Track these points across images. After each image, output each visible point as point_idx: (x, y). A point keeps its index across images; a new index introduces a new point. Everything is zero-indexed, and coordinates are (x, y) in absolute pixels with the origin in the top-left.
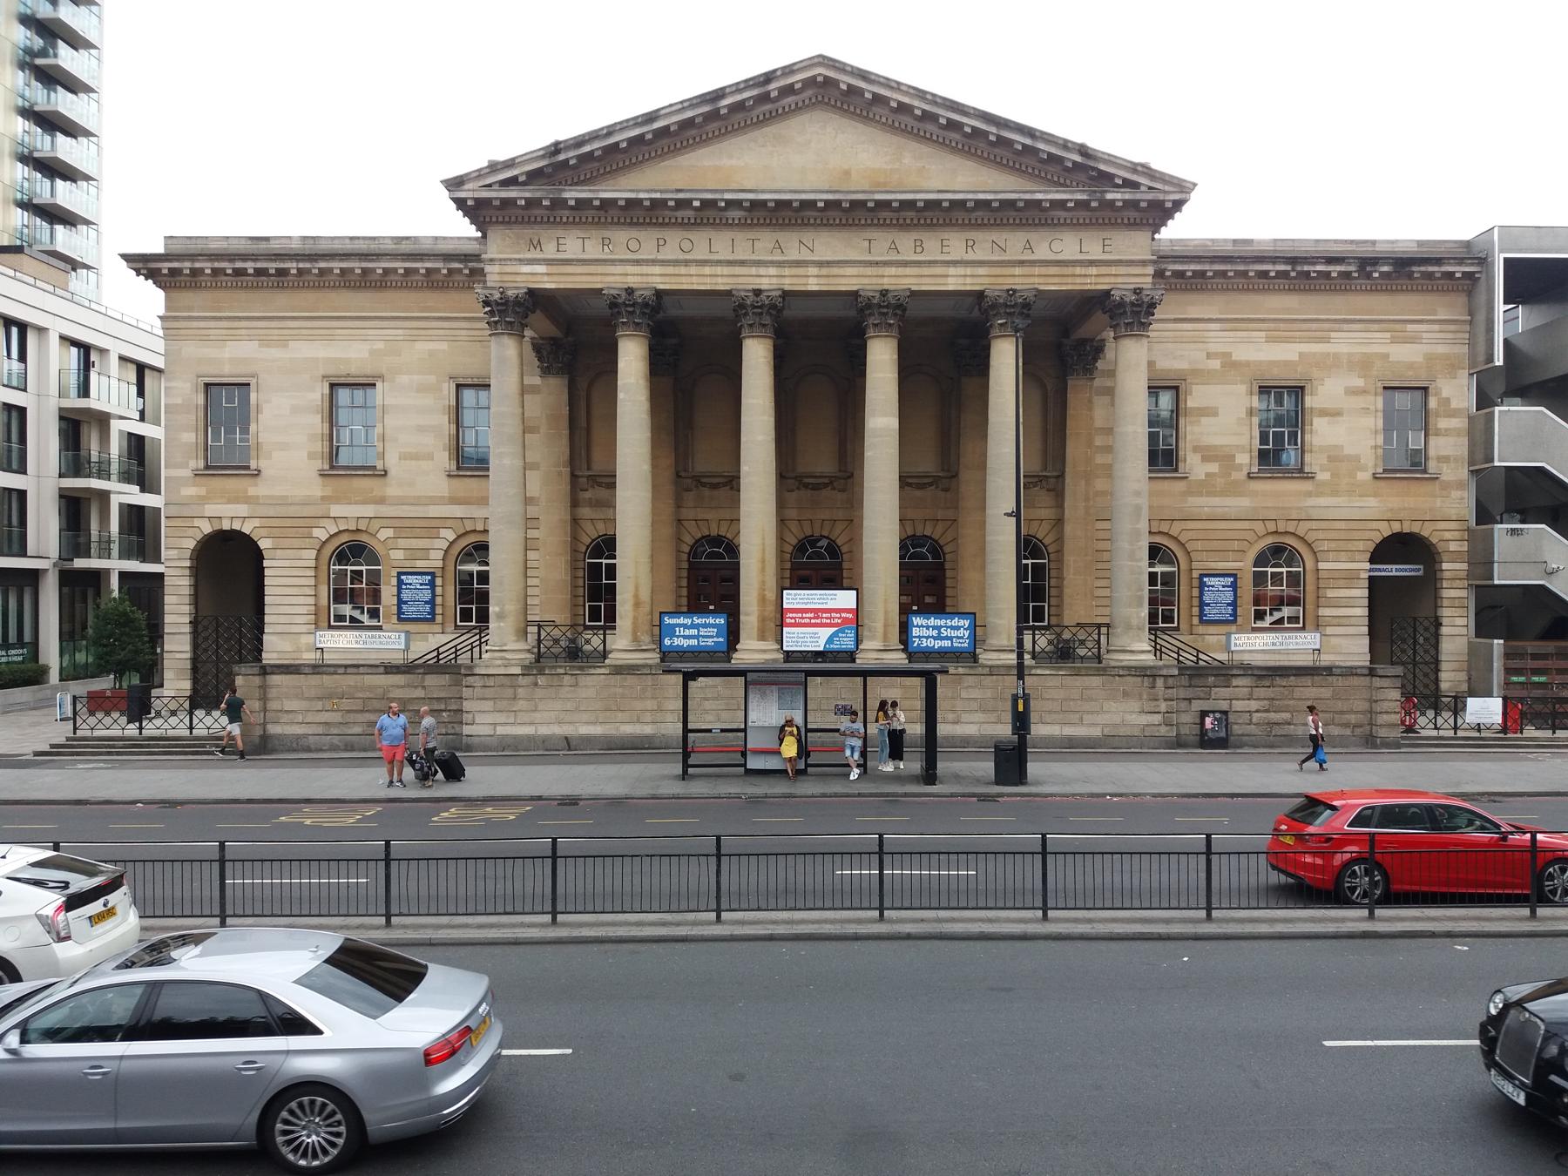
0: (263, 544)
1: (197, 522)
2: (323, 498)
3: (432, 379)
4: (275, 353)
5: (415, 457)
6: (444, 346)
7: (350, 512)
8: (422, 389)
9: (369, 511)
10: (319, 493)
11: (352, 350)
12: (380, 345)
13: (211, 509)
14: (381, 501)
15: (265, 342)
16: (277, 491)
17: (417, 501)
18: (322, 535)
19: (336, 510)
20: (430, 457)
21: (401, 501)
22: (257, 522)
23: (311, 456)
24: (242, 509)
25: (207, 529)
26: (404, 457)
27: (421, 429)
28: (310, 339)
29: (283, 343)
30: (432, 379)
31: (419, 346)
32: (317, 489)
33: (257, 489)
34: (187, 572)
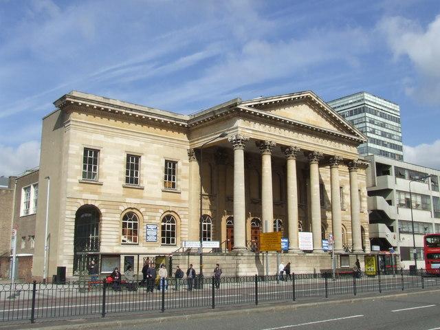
0: (102, 211)
1: (79, 201)
2: (123, 195)
3: (158, 157)
4: (110, 140)
5: (153, 183)
6: (162, 146)
7: (132, 201)
8: (155, 160)
9: (138, 201)
10: (122, 193)
11: (135, 145)
12: (143, 143)
13: (85, 196)
14: (142, 198)
15: (106, 135)
16: (109, 191)
17: (153, 199)
18: (122, 209)
19: (128, 200)
20: (157, 184)
21: (148, 198)
22: (100, 202)
23: (120, 179)
24: (96, 197)
25: (82, 204)
26: (149, 183)
27: (155, 174)
28: (122, 137)
29: (112, 137)
30: (158, 157)
31: (155, 145)
32: (121, 191)
33: (103, 189)
34: (74, 220)
